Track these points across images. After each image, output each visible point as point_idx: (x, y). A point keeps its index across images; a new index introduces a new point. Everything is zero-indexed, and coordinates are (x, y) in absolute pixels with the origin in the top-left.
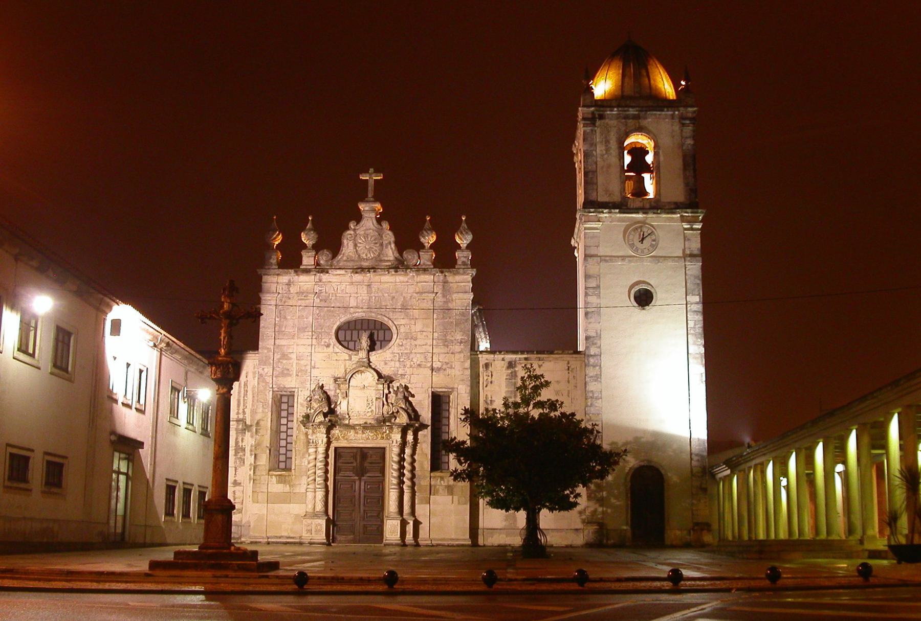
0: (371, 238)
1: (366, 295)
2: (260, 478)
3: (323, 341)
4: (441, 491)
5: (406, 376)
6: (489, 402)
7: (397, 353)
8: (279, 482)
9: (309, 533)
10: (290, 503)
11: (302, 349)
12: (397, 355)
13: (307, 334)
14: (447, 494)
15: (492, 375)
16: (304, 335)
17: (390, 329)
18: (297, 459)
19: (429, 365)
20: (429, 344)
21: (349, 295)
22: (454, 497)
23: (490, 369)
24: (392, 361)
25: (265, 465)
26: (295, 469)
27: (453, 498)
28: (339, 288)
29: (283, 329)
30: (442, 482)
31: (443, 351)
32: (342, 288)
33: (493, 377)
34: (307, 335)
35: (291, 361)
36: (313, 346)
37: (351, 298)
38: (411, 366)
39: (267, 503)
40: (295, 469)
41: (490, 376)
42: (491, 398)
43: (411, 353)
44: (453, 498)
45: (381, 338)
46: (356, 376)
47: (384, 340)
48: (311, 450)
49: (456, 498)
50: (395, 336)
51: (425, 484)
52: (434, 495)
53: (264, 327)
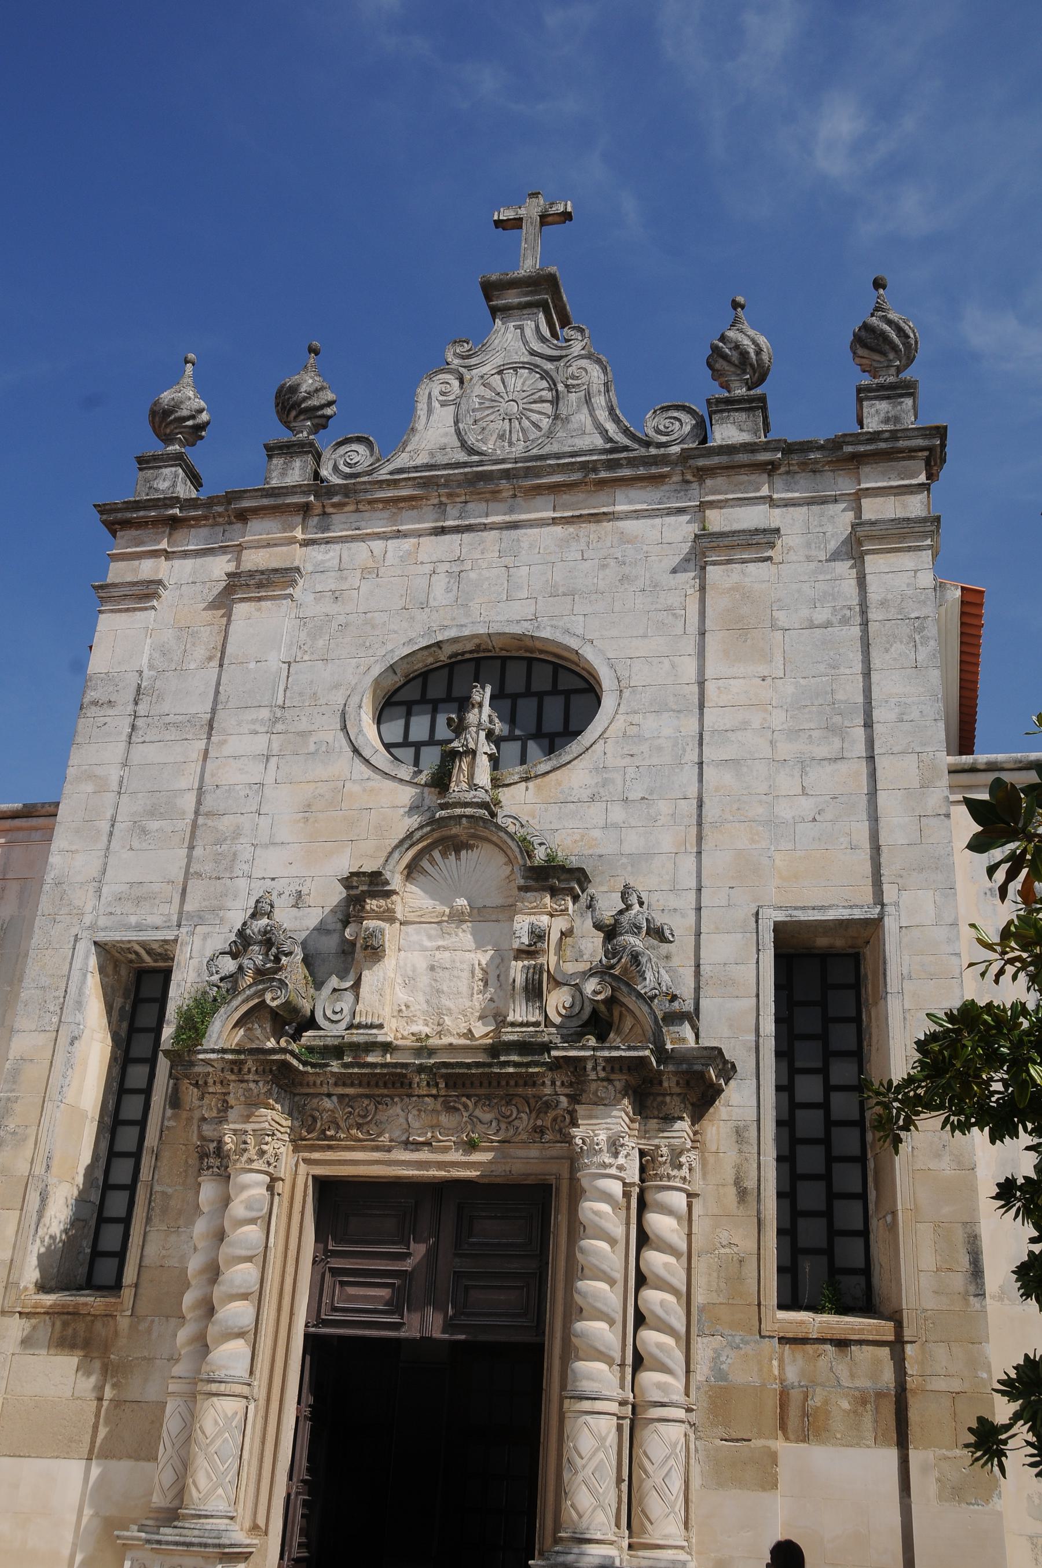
0: (523, 384)
3: (313, 739)
4: (838, 1424)
12: (618, 777)
14: (871, 1442)
18: (152, 1236)
21: (428, 568)
24: (592, 799)
26: (136, 1285)
31: (822, 751)
34: (254, 721)
36: (273, 761)
37: (435, 578)
40: (136, 1285)
46: (432, 862)
48: (208, 1191)
50: (608, 702)
51: (754, 1379)
52: (804, 1438)
53: (95, 703)
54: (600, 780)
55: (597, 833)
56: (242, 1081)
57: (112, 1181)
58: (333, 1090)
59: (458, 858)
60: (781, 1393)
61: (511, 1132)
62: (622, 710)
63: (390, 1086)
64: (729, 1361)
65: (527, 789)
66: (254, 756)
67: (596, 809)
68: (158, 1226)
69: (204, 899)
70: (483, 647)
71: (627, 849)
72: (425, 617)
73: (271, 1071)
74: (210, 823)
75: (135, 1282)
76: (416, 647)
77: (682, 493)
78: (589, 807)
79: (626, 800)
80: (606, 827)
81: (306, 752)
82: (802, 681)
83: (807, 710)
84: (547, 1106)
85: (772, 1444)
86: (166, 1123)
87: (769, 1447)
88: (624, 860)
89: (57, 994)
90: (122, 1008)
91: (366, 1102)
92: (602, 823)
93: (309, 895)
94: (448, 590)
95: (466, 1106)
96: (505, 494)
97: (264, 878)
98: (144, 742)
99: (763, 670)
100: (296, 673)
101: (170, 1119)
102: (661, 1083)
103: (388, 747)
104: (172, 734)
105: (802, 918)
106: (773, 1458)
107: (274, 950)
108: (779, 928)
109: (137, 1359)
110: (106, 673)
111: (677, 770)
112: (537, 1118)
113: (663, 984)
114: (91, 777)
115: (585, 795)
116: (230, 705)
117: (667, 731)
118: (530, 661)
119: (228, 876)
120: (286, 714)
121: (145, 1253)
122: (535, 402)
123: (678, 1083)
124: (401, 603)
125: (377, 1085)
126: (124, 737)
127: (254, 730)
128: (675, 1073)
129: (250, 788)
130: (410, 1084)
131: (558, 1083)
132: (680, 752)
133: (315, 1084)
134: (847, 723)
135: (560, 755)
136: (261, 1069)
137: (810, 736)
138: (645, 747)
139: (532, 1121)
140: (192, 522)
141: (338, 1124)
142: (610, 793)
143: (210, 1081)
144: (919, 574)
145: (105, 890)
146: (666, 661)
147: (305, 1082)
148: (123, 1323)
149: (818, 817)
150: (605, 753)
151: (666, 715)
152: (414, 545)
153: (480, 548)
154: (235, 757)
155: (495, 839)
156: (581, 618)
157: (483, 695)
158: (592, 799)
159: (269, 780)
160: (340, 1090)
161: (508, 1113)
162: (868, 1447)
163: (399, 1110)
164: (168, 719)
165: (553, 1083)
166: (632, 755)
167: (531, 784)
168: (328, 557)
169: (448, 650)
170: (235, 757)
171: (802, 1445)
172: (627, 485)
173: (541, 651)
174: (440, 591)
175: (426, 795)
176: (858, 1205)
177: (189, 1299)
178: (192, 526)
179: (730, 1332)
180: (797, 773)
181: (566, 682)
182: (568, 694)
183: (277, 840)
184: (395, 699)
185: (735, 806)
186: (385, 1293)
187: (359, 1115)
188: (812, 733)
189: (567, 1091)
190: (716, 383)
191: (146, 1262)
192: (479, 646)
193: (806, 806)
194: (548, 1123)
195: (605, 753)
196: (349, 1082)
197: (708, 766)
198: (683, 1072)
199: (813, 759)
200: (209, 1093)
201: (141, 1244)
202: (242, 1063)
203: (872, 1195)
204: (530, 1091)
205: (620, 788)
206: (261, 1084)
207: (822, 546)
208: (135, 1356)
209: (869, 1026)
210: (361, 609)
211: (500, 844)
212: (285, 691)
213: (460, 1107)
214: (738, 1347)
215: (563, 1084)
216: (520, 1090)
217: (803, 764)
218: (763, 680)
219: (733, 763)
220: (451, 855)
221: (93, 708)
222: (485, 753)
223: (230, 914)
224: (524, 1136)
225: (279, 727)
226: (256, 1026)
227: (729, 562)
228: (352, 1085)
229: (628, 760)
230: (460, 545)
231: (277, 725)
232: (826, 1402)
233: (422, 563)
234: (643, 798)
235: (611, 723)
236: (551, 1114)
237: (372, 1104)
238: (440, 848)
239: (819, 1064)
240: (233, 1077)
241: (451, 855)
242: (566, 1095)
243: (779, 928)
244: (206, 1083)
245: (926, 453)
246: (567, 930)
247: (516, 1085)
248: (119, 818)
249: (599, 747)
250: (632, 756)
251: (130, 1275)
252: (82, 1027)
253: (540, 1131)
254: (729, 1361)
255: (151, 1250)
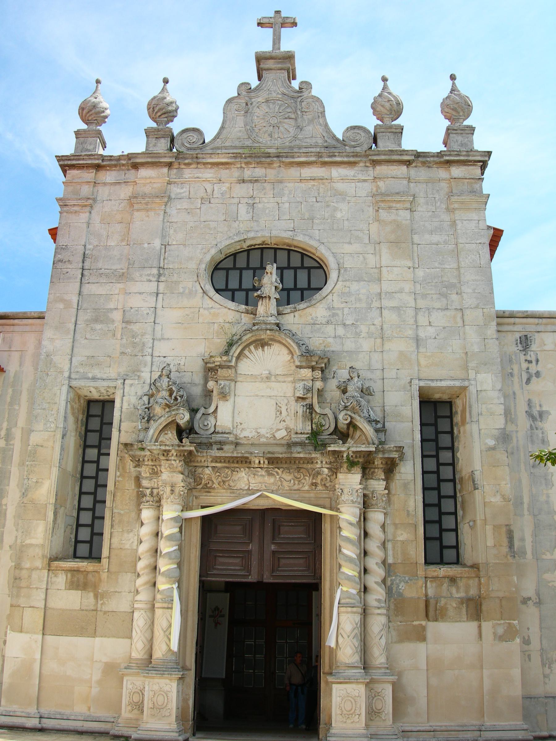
0: (279, 109)
1: (272, 200)
2: (30, 576)
3: (181, 285)
4: (451, 612)
5: (361, 356)
6: (536, 413)
7: (338, 309)
8: (73, 585)
9: (136, 711)
10: (94, 635)
11: (135, 302)
13: (148, 271)
14: (465, 619)
15: (537, 361)
16: (141, 276)
17: (321, 267)
18: (115, 534)
19: (410, 333)
20: (407, 290)
21: (236, 201)
22: (485, 625)
23: (534, 347)
24: (328, 323)
25: (43, 546)
26: (109, 558)
27: (480, 627)
28: (216, 189)
29: (100, 265)
30: (454, 590)
31: (437, 305)
32: (224, 189)
33: (539, 363)
34: (149, 275)
35: (112, 327)
36: (160, 296)
38: (370, 335)
39: (43, 634)
40: (109, 558)
41: (534, 363)
42: (540, 406)
43: (370, 308)
44: (480, 627)
45: (302, 282)
46: (250, 351)
47: (309, 288)
48: (147, 514)
49: (487, 626)
50: (333, 276)
52: (436, 620)
54: (331, 314)
55: (331, 340)
56: (167, 460)
57: (82, 506)
58: (209, 465)
59: (263, 350)
60: (426, 601)
61: (301, 486)
62: (340, 279)
63: (240, 463)
64: (403, 588)
65: (294, 316)
66: (151, 293)
67: (330, 329)
68: (117, 529)
69: (129, 366)
70: (266, 242)
71: (346, 349)
72: (236, 226)
73: (184, 455)
74: (129, 327)
75: (108, 556)
76: (233, 241)
77: (365, 172)
78: (326, 327)
79: (344, 325)
80: (335, 337)
81: (178, 292)
82: (427, 270)
83: (430, 284)
84: (319, 473)
85: (424, 623)
86: (117, 479)
87: (422, 624)
88: (345, 354)
89: (53, 413)
90: (82, 420)
91: (227, 470)
92: (333, 335)
93: (184, 365)
94: (248, 212)
95: (277, 473)
96: (275, 165)
97: (159, 356)
98: (89, 283)
99: (410, 264)
100: (169, 251)
101: (119, 477)
102: (374, 463)
103: (217, 291)
104: (103, 280)
105: (432, 385)
106: (424, 628)
107: (175, 394)
108: (421, 389)
109: (112, 592)
110: (66, 246)
111: (369, 311)
112: (313, 479)
113: (371, 415)
114: (62, 300)
115: (324, 321)
116: (135, 266)
117: (363, 291)
118: (289, 251)
119: (140, 354)
120: (165, 272)
121: (111, 542)
122: (286, 118)
123: (382, 463)
124: (223, 218)
125: (233, 462)
126: (79, 280)
127: (149, 279)
128: (381, 458)
129: (149, 309)
130: (250, 462)
131: (324, 462)
132: (370, 302)
133: (201, 461)
134: (449, 292)
135: (311, 300)
136: (178, 454)
137: (432, 297)
138: (353, 299)
139: (311, 480)
140: (108, 168)
141: (213, 481)
142: (337, 320)
143: (146, 459)
144: (480, 221)
145: (74, 359)
146: (361, 256)
147: (196, 460)
148: (104, 576)
149: (437, 337)
150: (333, 301)
151: (362, 283)
152: (228, 188)
153: (263, 192)
154: (140, 293)
155: (284, 342)
156: (317, 232)
157: (272, 269)
158: (328, 323)
159: (159, 306)
160: (214, 464)
161: (299, 476)
162: (464, 621)
163: (243, 474)
164: (101, 271)
165: (322, 462)
166: (346, 302)
167: (297, 314)
168: (182, 191)
169: (249, 243)
170: (140, 293)
171: (435, 623)
172: (337, 166)
173: (295, 247)
174: (243, 211)
175: (243, 317)
176: (453, 517)
177: (141, 565)
178: (108, 170)
179: (403, 576)
180: (426, 315)
181: (308, 263)
182: (309, 269)
183: (165, 337)
184: (219, 267)
185: (398, 330)
186: (238, 561)
187: (224, 477)
188: (433, 295)
189: (328, 466)
190: (375, 117)
191: (113, 546)
192: (264, 242)
193: (431, 331)
194: (319, 481)
195: (333, 301)
196: (219, 461)
197: (384, 309)
198: (385, 458)
199: (434, 308)
200: (145, 465)
201: (109, 537)
202: (169, 451)
203: (460, 513)
204: (310, 466)
205: (341, 318)
206: (178, 461)
207: (434, 204)
208: (111, 590)
209: (458, 436)
210: (202, 220)
211: (287, 344)
212: (164, 260)
213: (275, 474)
214: (407, 582)
215: (326, 462)
216: (305, 466)
217: (429, 310)
218: (409, 269)
219: (397, 309)
220: (259, 348)
221: (60, 263)
222: (275, 298)
223: (143, 374)
224: (307, 488)
225: (162, 278)
226: (169, 432)
227: (390, 208)
228: (220, 462)
229: (344, 305)
230: (253, 190)
231: (161, 278)
232: (446, 604)
233: (233, 197)
234: (353, 324)
235: (335, 286)
236: (320, 477)
237: (230, 472)
238: (254, 345)
239: (434, 453)
240: (164, 458)
241: (259, 348)
242: (327, 468)
243: (421, 389)
244: (144, 460)
245: (481, 164)
246: (321, 388)
247: (304, 463)
248: (78, 322)
249: (330, 297)
250: (346, 302)
251: (105, 552)
252: (66, 429)
253: (315, 485)
254: (403, 588)
255: (115, 541)
